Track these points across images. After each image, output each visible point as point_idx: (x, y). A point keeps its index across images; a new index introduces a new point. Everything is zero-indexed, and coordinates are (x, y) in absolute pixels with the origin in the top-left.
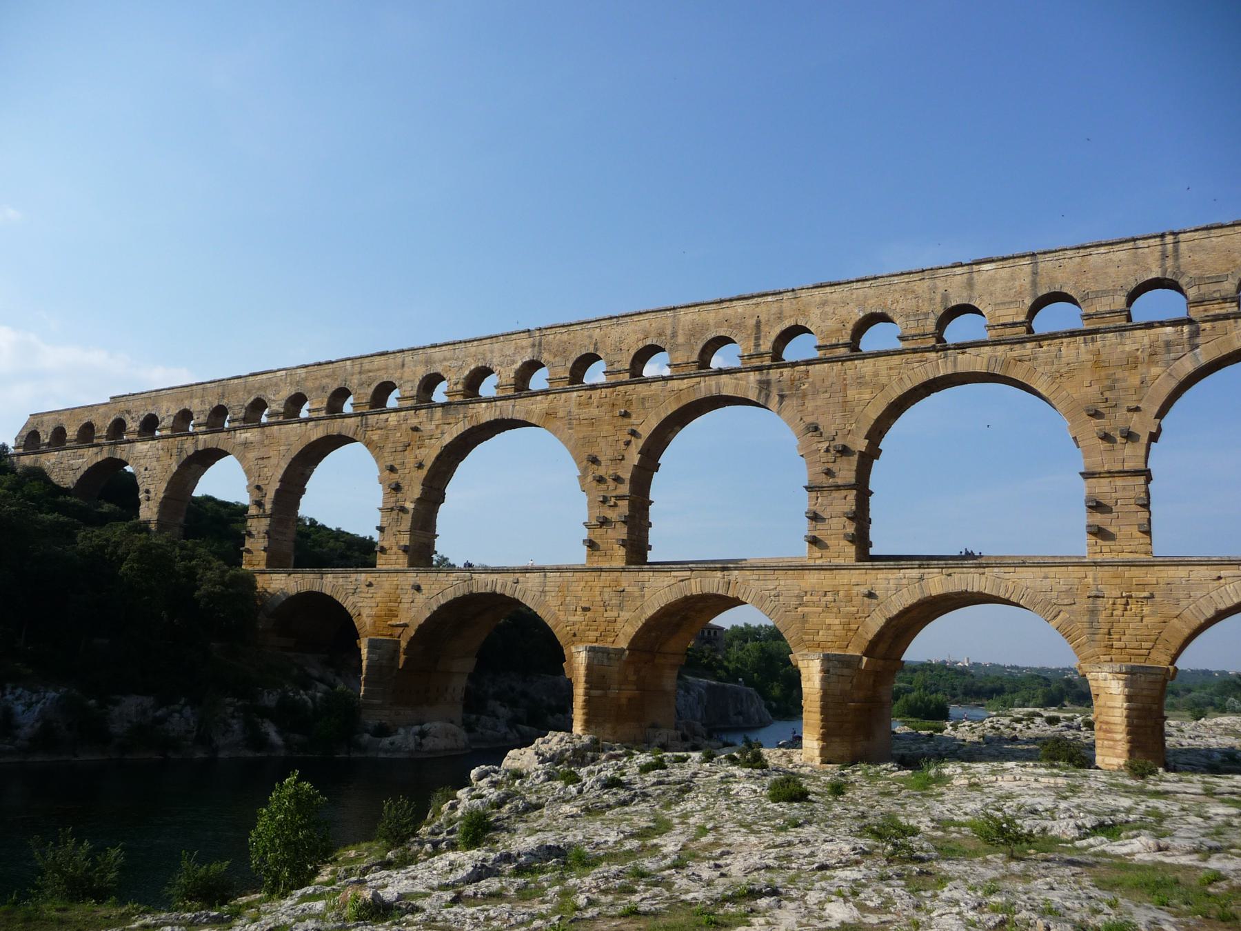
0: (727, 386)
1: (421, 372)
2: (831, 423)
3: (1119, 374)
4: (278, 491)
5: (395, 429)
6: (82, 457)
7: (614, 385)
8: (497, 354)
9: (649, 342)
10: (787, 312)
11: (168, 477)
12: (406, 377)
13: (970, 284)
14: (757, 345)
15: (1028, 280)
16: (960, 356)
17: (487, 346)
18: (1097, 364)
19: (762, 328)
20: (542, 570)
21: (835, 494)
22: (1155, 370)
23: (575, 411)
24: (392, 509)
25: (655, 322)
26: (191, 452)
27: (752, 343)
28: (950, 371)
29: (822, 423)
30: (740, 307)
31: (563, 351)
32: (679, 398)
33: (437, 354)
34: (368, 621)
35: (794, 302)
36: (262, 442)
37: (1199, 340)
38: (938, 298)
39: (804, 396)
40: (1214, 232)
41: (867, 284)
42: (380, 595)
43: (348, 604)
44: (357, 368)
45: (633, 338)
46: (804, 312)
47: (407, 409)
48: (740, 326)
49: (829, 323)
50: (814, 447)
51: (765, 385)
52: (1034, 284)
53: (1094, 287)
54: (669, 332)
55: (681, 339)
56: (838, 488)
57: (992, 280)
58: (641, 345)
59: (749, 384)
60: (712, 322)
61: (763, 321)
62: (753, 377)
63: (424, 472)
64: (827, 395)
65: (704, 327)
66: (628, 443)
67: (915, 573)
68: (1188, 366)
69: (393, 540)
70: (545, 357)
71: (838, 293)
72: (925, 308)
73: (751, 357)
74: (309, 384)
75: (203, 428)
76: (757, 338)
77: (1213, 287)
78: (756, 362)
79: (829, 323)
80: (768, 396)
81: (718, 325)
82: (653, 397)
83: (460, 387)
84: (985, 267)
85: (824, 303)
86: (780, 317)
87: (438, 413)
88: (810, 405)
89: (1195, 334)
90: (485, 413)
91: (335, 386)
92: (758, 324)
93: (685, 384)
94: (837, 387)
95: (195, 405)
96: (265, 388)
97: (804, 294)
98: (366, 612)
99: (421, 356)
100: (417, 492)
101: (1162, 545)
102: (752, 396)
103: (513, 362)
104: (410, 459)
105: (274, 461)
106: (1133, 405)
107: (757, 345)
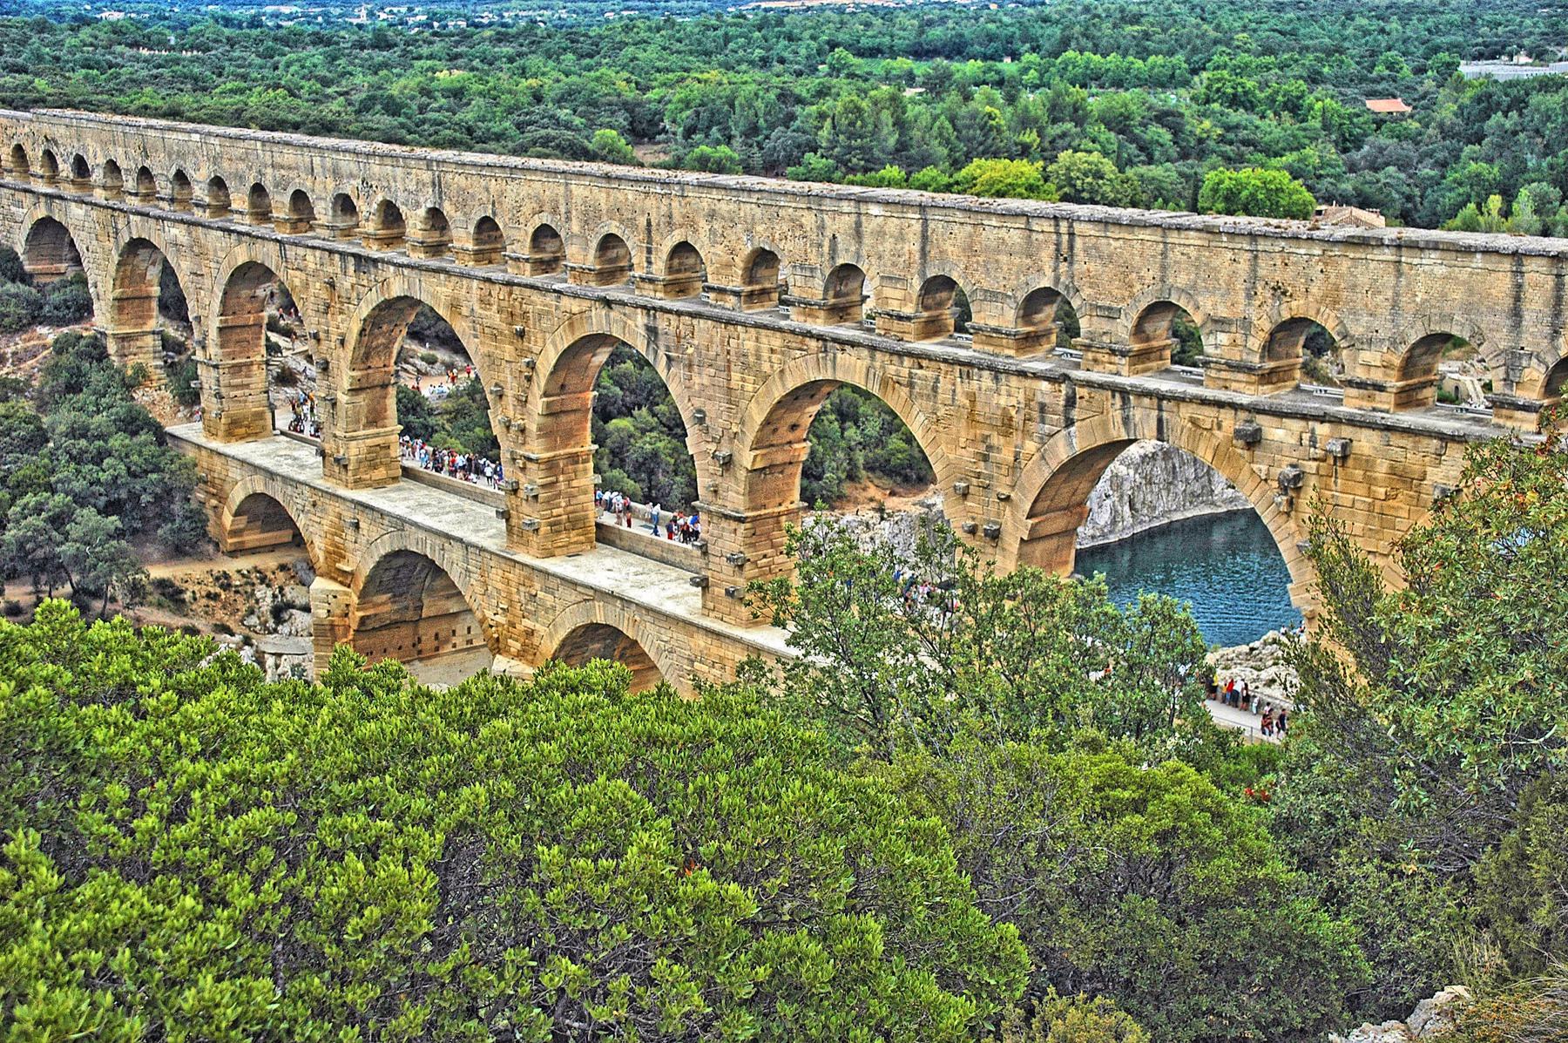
3: (996, 440)
6: (20, 205)
10: (677, 218)
11: (112, 268)
15: (916, 248)
19: (656, 237)
22: (1031, 446)
29: (711, 409)
37: (1075, 414)
40: (1114, 232)
51: (652, 331)
54: (563, 209)
57: (880, 234)
62: (641, 319)
64: (712, 371)
66: (529, 379)
77: (1106, 326)
79: (719, 249)
85: (712, 215)
89: (1071, 402)
92: (649, 223)
94: (721, 363)
103: (418, 205)
106: (1006, 492)
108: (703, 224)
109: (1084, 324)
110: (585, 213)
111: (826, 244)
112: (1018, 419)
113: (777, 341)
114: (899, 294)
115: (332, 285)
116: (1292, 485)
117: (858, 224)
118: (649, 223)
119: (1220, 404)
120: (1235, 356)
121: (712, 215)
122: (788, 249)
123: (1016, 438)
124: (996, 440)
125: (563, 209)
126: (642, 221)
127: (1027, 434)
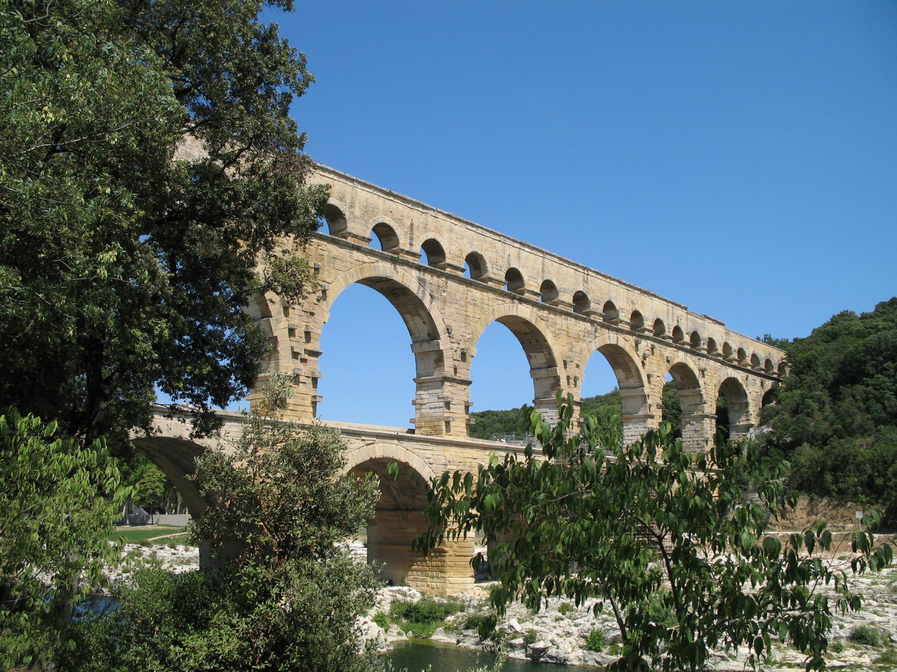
3: (574, 343)
10: (430, 227)
13: (519, 257)
14: (411, 245)
15: (541, 267)
16: (519, 306)
21: (459, 386)
22: (585, 345)
27: (408, 241)
28: (515, 314)
29: (454, 326)
32: (361, 270)
35: (435, 220)
37: (597, 335)
38: (506, 260)
39: (445, 301)
41: (474, 229)
46: (439, 231)
49: (454, 248)
50: (450, 345)
51: (422, 282)
52: (543, 271)
53: (564, 286)
54: (348, 200)
60: (381, 208)
61: (415, 225)
62: (415, 273)
64: (457, 306)
71: (459, 228)
72: (500, 263)
73: (408, 253)
76: (411, 239)
80: (424, 292)
84: (527, 249)
88: (447, 310)
92: (412, 225)
94: (463, 303)
97: (440, 216)
107: (411, 245)
109: (592, 304)
110: (366, 207)
111: (506, 257)
113: (491, 295)
114: (535, 284)
117: (519, 253)
118: (412, 225)
121: (451, 231)
122: (488, 256)
123: (580, 343)
124: (574, 343)
125: (348, 200)
126: (408, 222)
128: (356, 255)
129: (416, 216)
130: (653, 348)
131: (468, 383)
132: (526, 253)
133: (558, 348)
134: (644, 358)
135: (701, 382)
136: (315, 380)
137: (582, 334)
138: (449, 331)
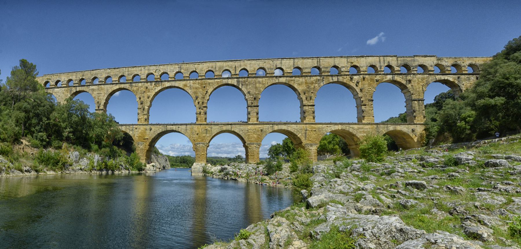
0: (230, 81)
1: (147, 72)
2: (253, 91)
3: (310, 85)
4: (105, 103)
5: (141, 87)
7: (202, 79)
8: (169, 69)
9: (210, 69)
12: (142, 73)
17: (165, 67)
18: (306, 83)
19: (237, 68)
20: (186, 125)
22: (316, 85)
23: (192, 85)
24: (141, 109)
25: (211, 64)
26: (75, 91)
29: (251, 91)
30: (231, 63)
31: (187, 70)
32: (218, 84)
33: (152, 68)
34: (137, 138)
36: (98, 89)
39: (247, 85)
42: (140, 131)
43: (131, 133)
44: (127, 70)
45: (205, 68)
46: (246, 66)
47: (144, 82)
48: (231, 67)
51: (238, 82)
55: (217, 69)
56: (255, 106)
58: (207, 70)
59: (234, 82)
62: (236, 80)
63: (150, 99)
65: (223, 67)
67: (271, 125)
68: (322, 84)
69: (142, 117)
70: (182, 71)
71: (253, 62)
74: (112, 74)
75: (77, 85)
78: (236, 76)
81: (226, 66)
82: (212, 83)
83: (159, 77)
85: (251, 64)
86: (240, 66)
87: (153, 83)
88: (248, 87)
89: (323, 78)
90: (167, 84)
91: (120, 75)
92: (235, 67)
93: (219, 80)
95: (73, 78)
96: (97, 74)
98: (136, 135)
99: (147, 68)
100: (149, 104)
101: (317, 120)
102: (236, 84)
104: (146, 95)
105: (103, 95)
108: (248, 66)
112: (314, 82)
115: (147, 88)
116: (358, 83)
119: (347, 75)
120: (346, 70)
124: (310, 85)
127: (316, 83)
128: (216, 80)
129: (237, 64)
130: (364, 78)
131: (258, 106)
132: (284, 61)
133: (300, 89)
134: (358, 83)
135: (409, 86)
136: (206, 113)
137: (314, 82)
138: (249, 93)
